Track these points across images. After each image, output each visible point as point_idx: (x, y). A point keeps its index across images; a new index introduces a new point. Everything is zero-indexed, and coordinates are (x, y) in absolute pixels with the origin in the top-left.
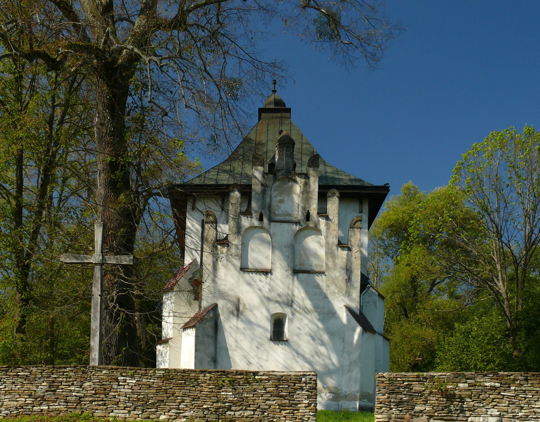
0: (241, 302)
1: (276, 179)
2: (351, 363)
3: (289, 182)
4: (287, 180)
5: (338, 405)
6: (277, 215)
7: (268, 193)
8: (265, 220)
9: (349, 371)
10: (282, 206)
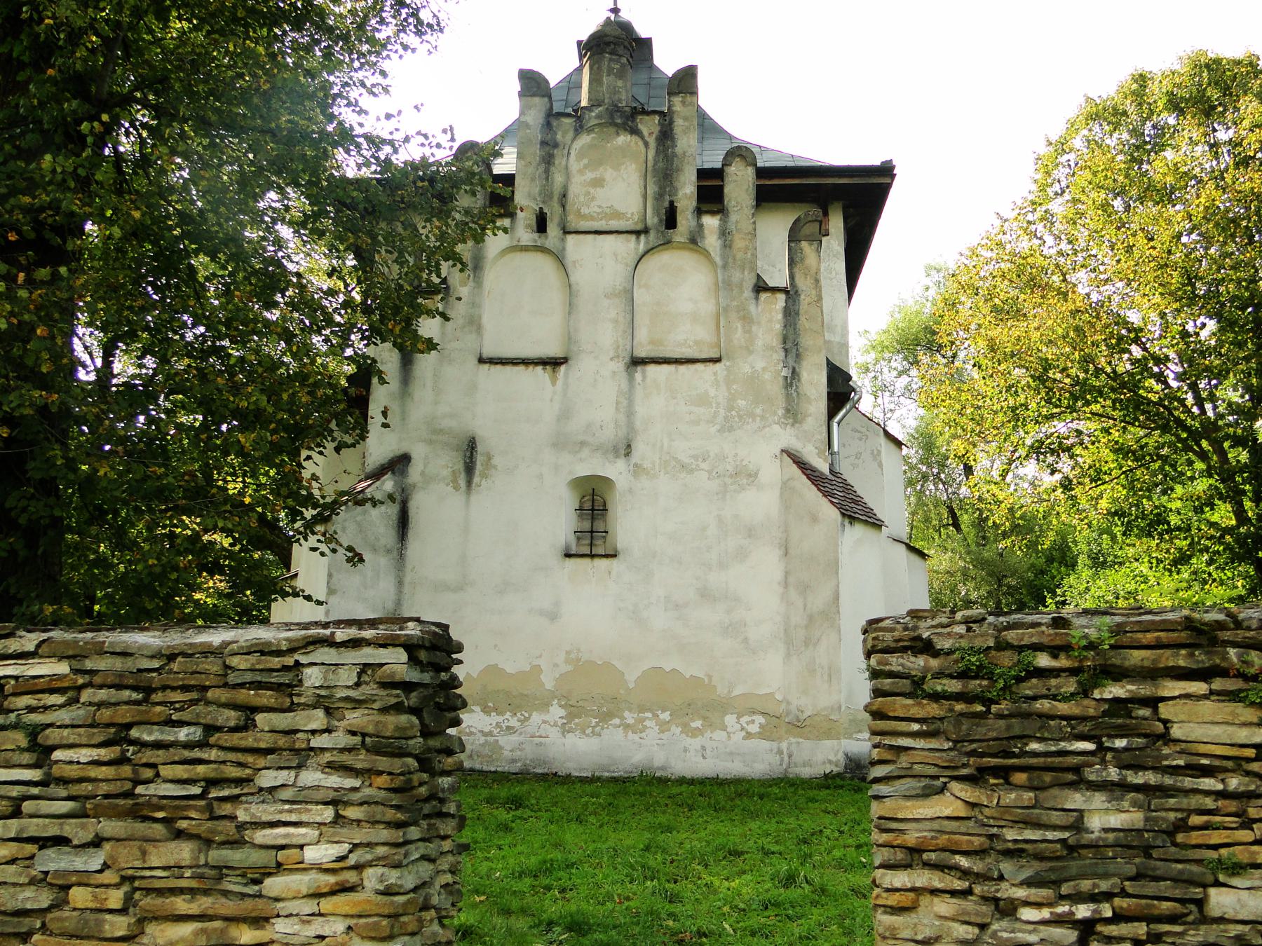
0: (480, 448)
1: (581, 127)
2: (811, 618)
3: (618, 134)
4: (612, 130)
5: (780, 752)
6: (584, 217)
7: (559, 161)
8: (553, 229)
9: (807, 642)
10: (600, 193)
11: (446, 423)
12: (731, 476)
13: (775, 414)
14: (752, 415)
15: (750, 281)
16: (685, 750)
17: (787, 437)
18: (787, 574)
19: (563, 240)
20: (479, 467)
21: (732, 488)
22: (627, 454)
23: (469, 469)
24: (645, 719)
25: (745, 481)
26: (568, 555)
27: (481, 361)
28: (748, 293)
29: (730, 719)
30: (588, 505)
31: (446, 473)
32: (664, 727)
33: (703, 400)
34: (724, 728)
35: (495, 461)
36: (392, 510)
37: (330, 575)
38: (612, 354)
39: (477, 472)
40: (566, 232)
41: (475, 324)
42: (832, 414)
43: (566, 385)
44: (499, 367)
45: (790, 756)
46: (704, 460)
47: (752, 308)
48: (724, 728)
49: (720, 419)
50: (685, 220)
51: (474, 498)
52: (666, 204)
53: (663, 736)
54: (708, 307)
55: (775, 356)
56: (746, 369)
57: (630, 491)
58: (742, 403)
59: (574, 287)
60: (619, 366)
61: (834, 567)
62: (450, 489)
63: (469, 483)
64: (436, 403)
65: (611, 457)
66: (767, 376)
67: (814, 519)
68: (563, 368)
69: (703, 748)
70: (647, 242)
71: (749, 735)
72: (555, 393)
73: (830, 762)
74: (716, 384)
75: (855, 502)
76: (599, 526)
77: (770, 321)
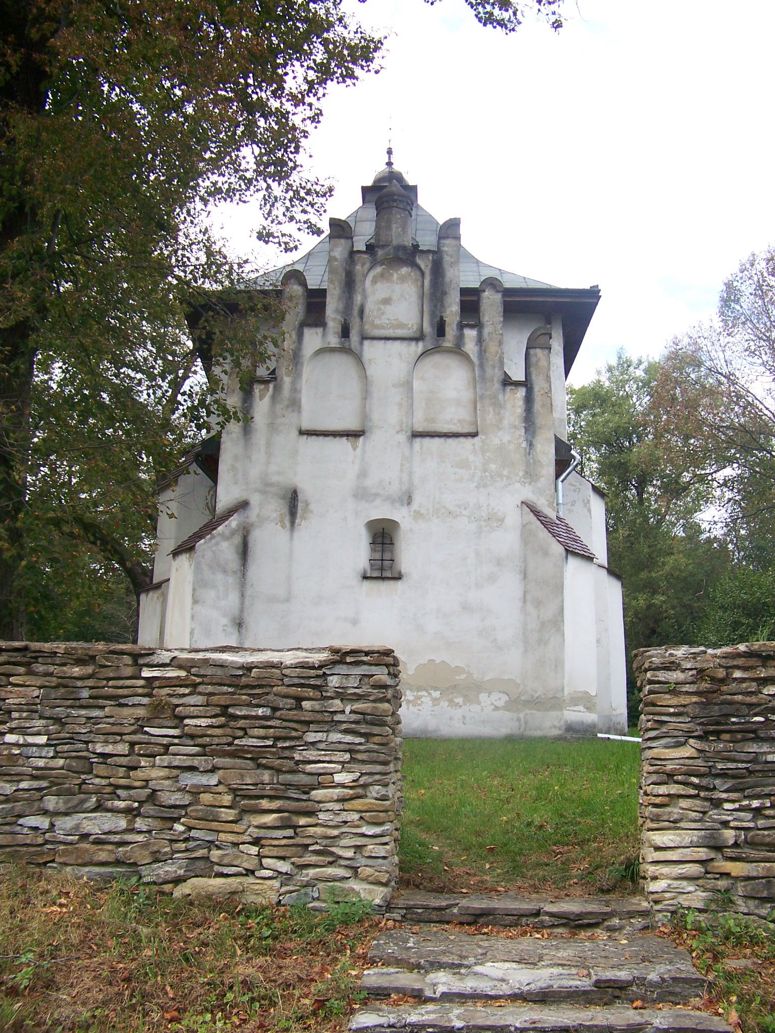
0: (300, 497)
1: (375, 260)
5: (519, 720)
8: (354, 337)
10: (388, 309)
11: (275, 479)
12: (485, 521)
13: (517, 475)
14: (501, 476)
15: (498, 376)
16: (451, 719)
17: (527, 493)
18: (525, 593)
19: (361, 344)
20: (300, 511)
21: (486, 529)
22: (409, 504)
23: (293, 512)
24: (421, 697)
25: (495, 524)
26: (365, 578)
27: (302, 433)
28: (497, 386)
29: (483, 696)
30: (380, 540)
31: (275, 515)
32: (435, 701)
33: (464, 464)
34: (479, 703)
35: (312, 507)
36: (237, 540)
37: (194, 590)
38: (398, 428)
39: (298, 515)
40: (364, 338)
41: (295, 404)
42: (557, 476)
43: (364, 452)
44: (314, 438)
45: (526, 723)
46: (465, 508)
47: (501, 397)
48: (479, 703)
49: (476, 479)
50: (451, 331)
51: (296, 534)
52: (438, 318)
53: (435, 708)
54: (467, 395)
55: (518, 432)
56: (497, 441)
57: (411, 530)
58: (493, 466)
59: (369, 378)
60: (402, 438)
61: (559, 588)
62: (279, 527)
63: (293, 523)
64: (268, 463)
65: (397, 505)
66: (511, 447)
67: (546, 553)
68: (361, 439)
69: (464, 717)
70: (424, 346)
71: (497, 708)
72: (355, 457)
73: (555, 727)
74: (474, 451)
75: (575, 541)
76: (387, 556)
77: (514, 406)
